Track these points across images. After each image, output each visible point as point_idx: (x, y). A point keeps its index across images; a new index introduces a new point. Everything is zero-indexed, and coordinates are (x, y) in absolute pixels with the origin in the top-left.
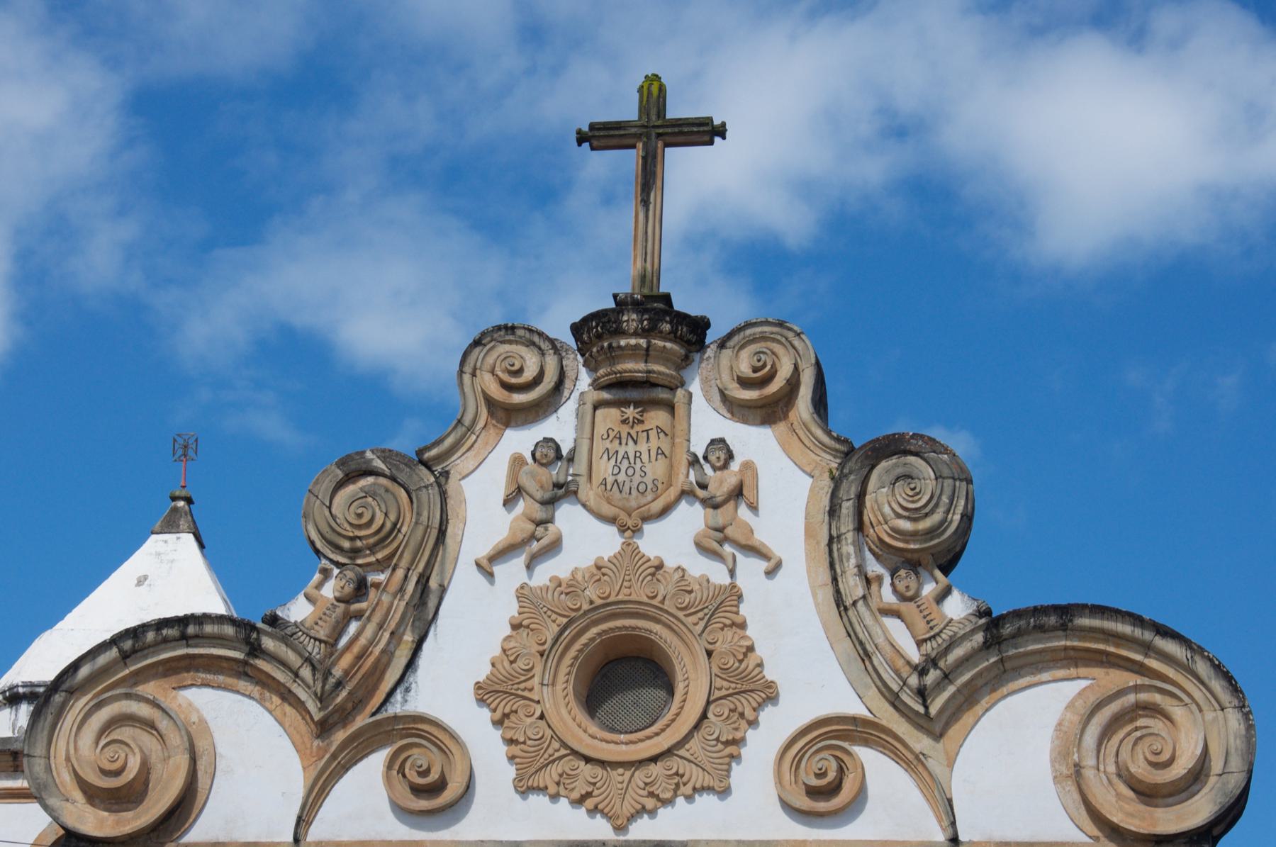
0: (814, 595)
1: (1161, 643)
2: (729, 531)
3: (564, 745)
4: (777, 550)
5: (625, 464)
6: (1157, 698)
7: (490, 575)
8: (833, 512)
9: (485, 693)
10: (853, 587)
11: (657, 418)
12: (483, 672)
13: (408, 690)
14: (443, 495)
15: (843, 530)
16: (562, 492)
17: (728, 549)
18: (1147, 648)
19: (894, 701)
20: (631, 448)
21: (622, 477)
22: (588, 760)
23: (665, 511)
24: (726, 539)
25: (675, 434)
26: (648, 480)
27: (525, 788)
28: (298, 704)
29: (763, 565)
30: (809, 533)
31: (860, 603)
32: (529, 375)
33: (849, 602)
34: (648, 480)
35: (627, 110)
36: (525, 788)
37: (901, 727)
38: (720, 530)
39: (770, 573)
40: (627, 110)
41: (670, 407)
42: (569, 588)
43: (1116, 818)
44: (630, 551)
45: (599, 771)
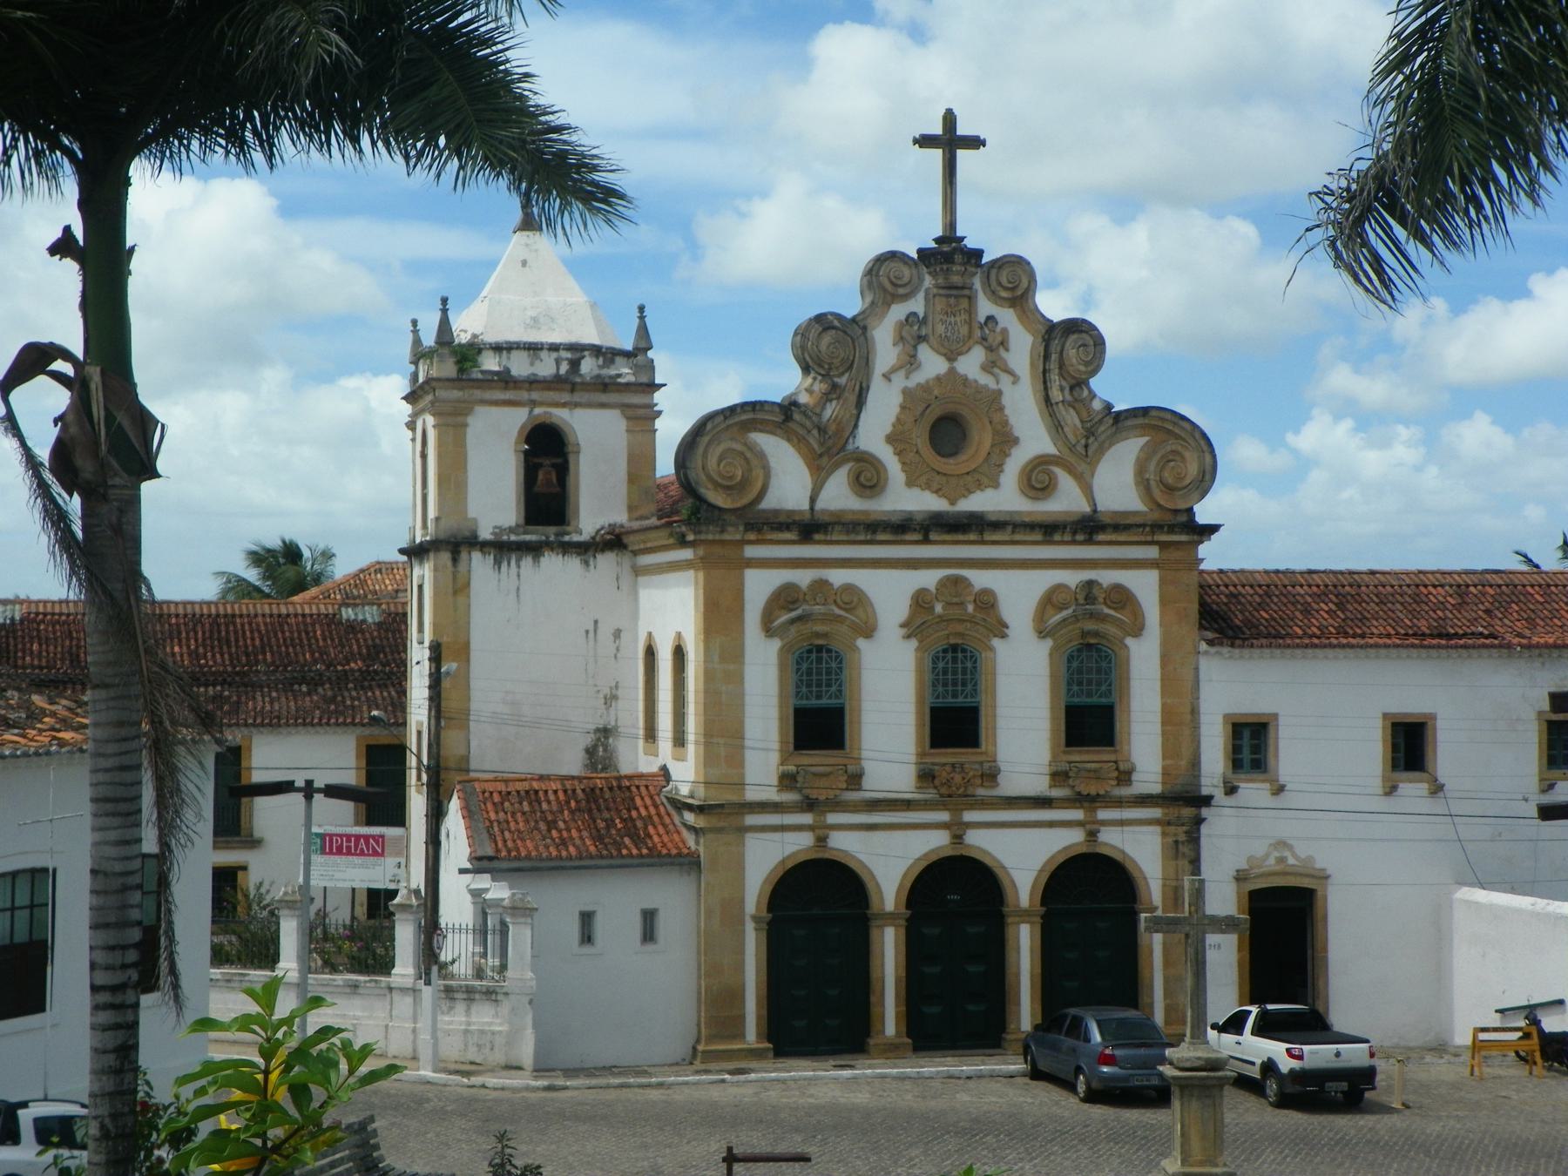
0: (1035, 395)
1: (1181, 423)
2: (998, 364)
3: (928, 465)
4: (1018, 372)
5: (950, 328)
6: (1179, 448)
7: (890, 380)
8: (1046, 357)
9: (891, 439)
10: (1056, 395)
11: (964, 303)
12: (889, 429)
13: (855, 437)
14: (866, 339)
15: (1052, 367)
16: (921, 339)
17: (996, 370)
18: (1175, 424)
19: (1072, 448)
20: (953, 319)
21: (949, 334)
22: (938, 473)
23: (969, 349)
24: (996, 366)
25: (971, 311)
26: (961, 336)
27: (910, 483)
28: (808, 444)
29: (1011, 379)
30: (1032, 365)
31: (1060, 405)
32: (906, 280)
33: (1053, 401)
34: (961, 336)
35: (937, 129)
36: (910, 483)
37: (1072, 459)
38: (993, 362)
39: (1014, 383)
40: (937, 129)
41: (970, 298)
42: (925, 388)
43: (1162, 503)
44: (952, 371)
45: (944, 478)
